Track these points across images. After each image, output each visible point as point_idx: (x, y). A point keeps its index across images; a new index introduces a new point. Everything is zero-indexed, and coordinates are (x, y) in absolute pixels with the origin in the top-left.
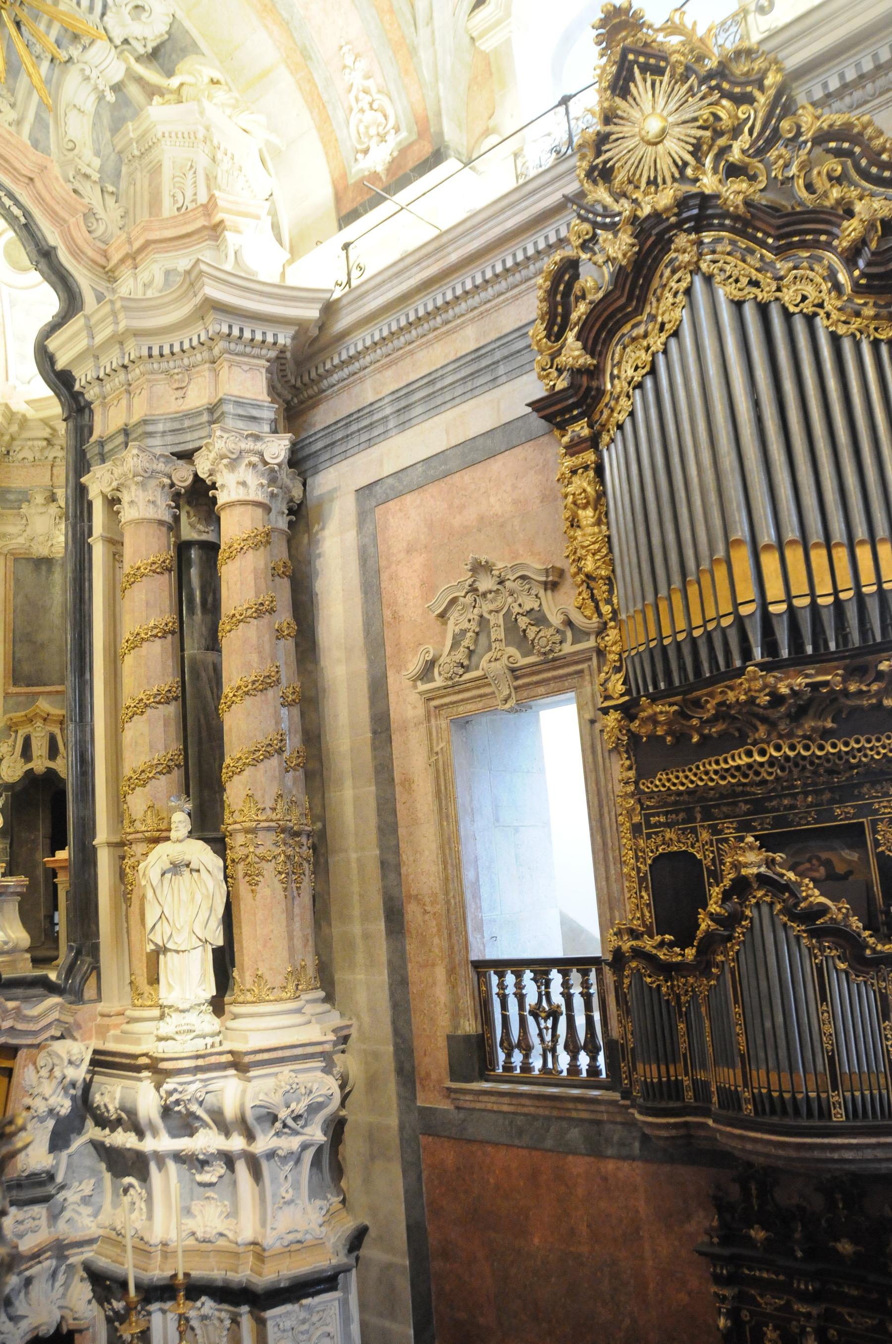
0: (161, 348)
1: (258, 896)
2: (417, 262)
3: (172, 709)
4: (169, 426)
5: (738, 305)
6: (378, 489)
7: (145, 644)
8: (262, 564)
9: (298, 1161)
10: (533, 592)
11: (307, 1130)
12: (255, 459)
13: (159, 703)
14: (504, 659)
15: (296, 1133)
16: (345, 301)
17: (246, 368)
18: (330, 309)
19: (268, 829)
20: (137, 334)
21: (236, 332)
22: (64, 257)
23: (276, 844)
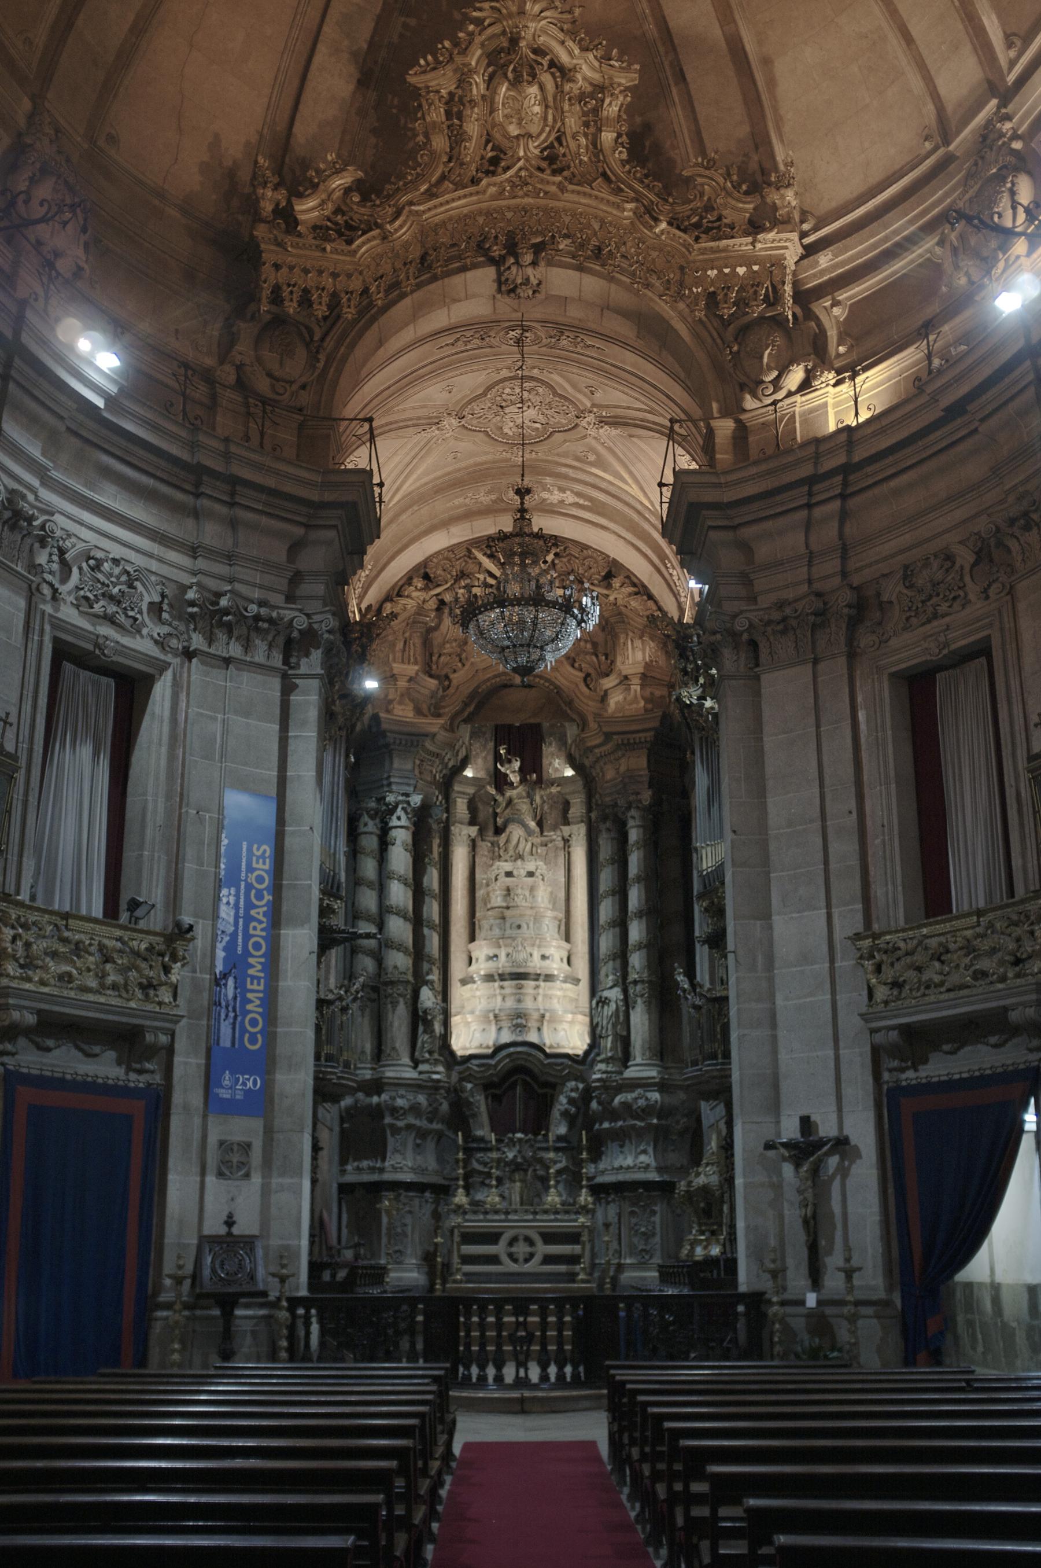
3: (617, 930)
5: (701, 738)
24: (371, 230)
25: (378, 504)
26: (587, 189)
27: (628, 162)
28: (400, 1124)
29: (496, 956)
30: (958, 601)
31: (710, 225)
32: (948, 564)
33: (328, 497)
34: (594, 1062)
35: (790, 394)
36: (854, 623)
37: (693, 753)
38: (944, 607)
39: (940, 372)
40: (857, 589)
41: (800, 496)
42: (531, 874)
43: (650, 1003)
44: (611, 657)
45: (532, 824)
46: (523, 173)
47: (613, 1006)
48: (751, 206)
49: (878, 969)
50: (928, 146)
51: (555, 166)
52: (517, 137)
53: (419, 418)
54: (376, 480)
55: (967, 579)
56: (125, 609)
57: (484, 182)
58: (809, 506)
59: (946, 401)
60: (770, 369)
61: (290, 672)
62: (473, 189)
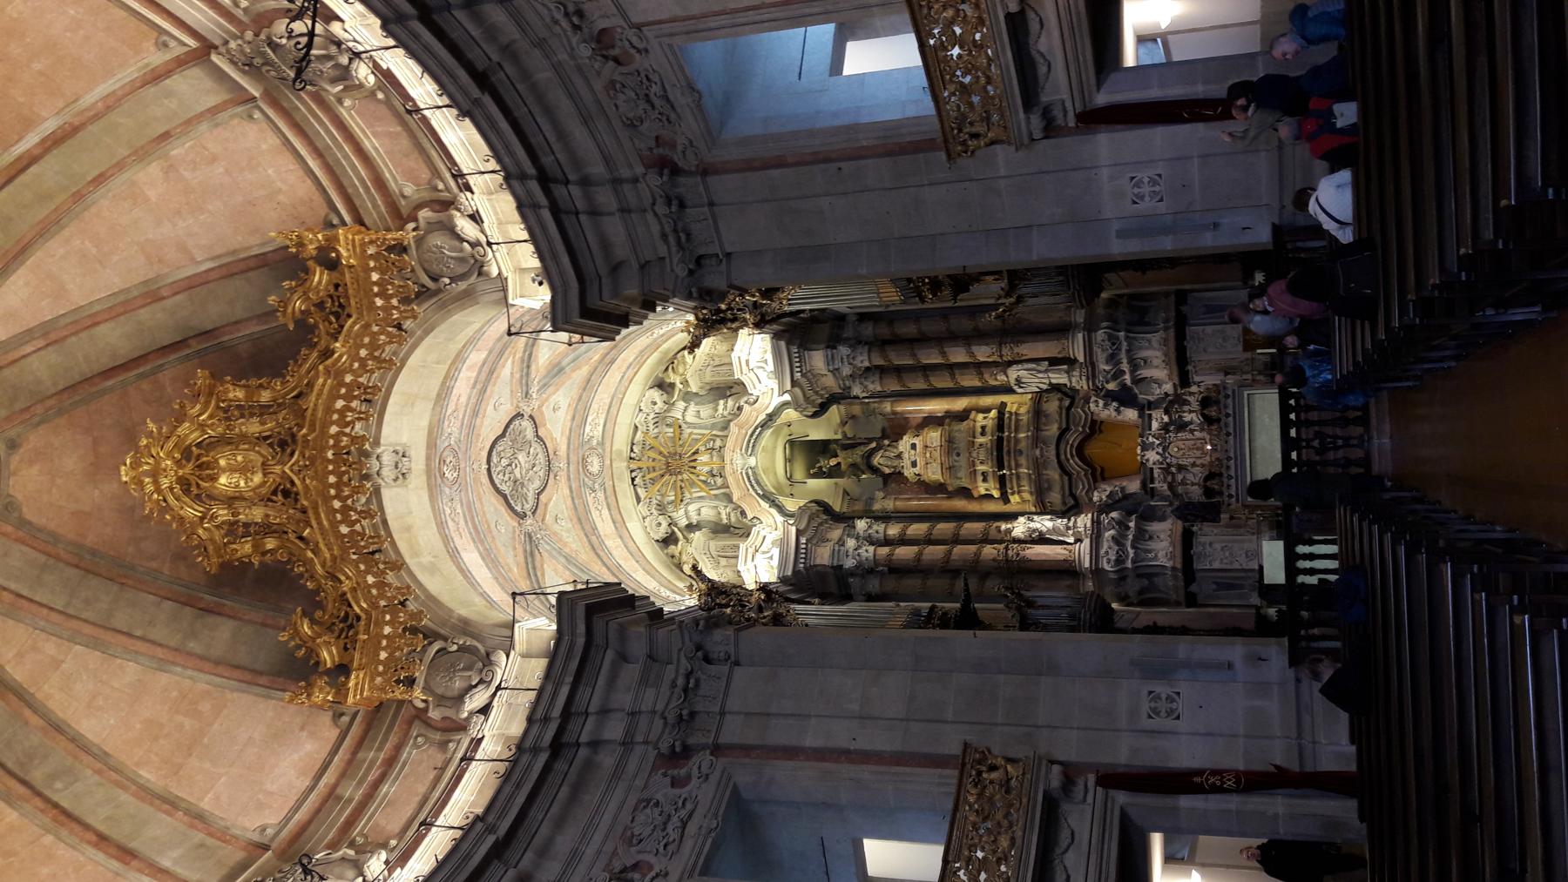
3: (957, 372)
8: (892, 353)
9: (1134, 338)
20: (804, 395)
21: (798, 369)
22: (770, 410)
24: (347, 600)
25: (590, 586)
26: (309, 412)
27: (284, 377)
28: (1131, 555)
29: (983, 473)
30: (651, 77)
31: (337, 304)
32: (618, 86)
33: (581, 628)
34: (1072, 389)
35: (483, 232)
36: (675, 171)
37: (803, 311)
38: (655, 89)
39: (450, 96)
40: (647, 167)
41: (568, 221)
42: (914, 446)
43: (1018, 342)
45: (874, 445)
46: (296, 468)
47: (1023, 373)
48: (318, 269)
49: (975, 136)
50: (257, 115)
51: (290, 441)
52: (265, 475)
53: (525, 551)
54: (569, 588)
55: (631, 68)
56: (676, 810)
57: (305, 503)
58: (577, 213)
59: (476, 92)
60: (461, 250)
61: (733, 659)
62: (311, 513)
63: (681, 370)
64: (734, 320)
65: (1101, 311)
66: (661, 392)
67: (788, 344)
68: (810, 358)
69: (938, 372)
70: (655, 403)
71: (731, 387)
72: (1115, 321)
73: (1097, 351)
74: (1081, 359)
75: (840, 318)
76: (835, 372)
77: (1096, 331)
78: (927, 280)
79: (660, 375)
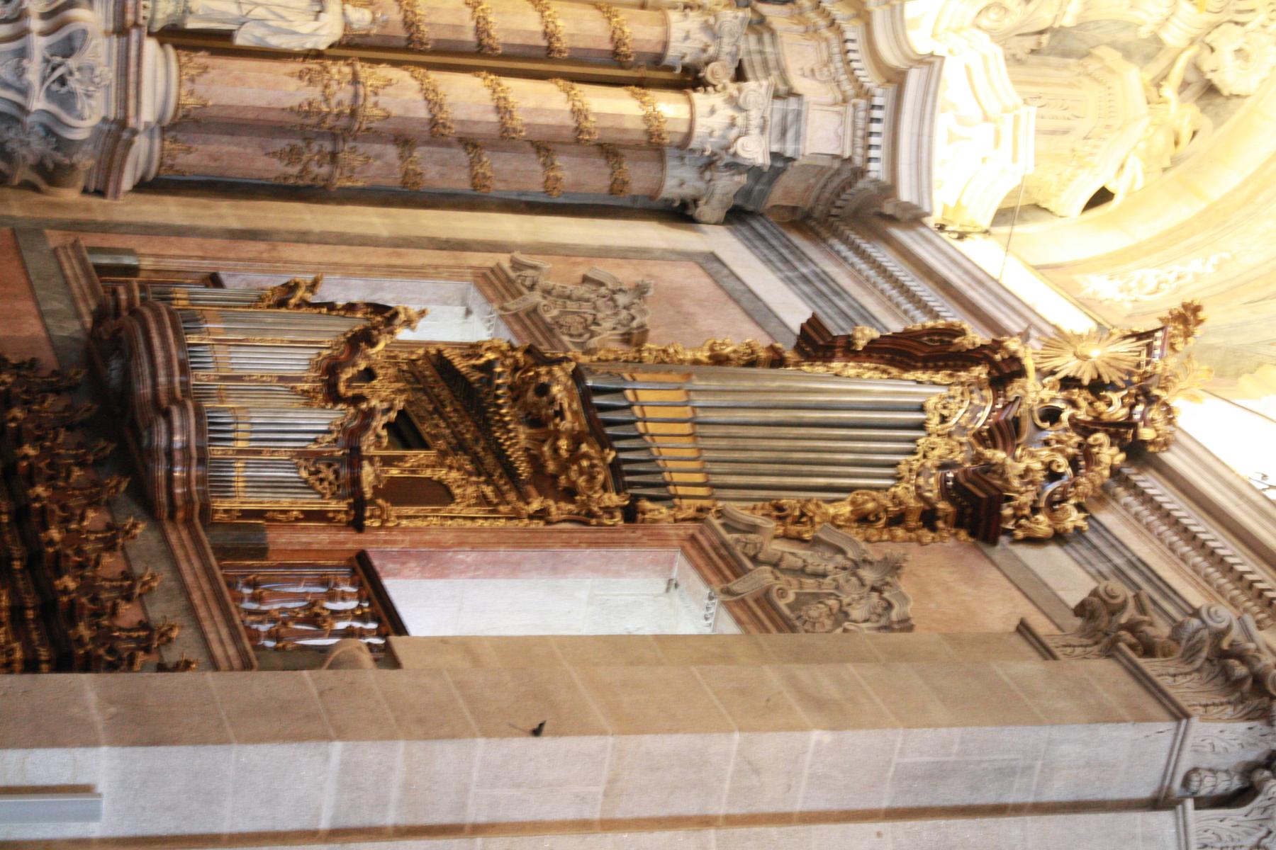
0: (854, 51)
1: (287, 78)
2: (967, 272)
3: (469, 36)
4: (771, 58)
5: (921, 409)
6: (716, 265)
7: (537, 14)
8: (628, 125)
10: (619, 327)
11: (42, 95)
12: (740, 121)
13: (478, 23)
14: (544, 302)
15: (44, 79)
16: (922, 230)
17: (840, 130)
18: (914, 218)
19: (356, 95)
20: (868, 26)
21: (876, 114)
23: (340, 103)
43: (307, 114)
44: (1034, 59)
47: (305, 25)
63: (1162, 140)
64: (1069, 383)
65: (85, 161)
66: (1216, 79)
67: (888, 189)
68: (840, 138)
69: (518, 41)
70: (1239, 51)
71: (1033, 51)
72: (49, 132)
73: (107, 73)
74: (151, 46)
75: (736, 216)
76: (786, 93)
77: (105, 120)
78: (563, 444)
79: (1206, 123)
